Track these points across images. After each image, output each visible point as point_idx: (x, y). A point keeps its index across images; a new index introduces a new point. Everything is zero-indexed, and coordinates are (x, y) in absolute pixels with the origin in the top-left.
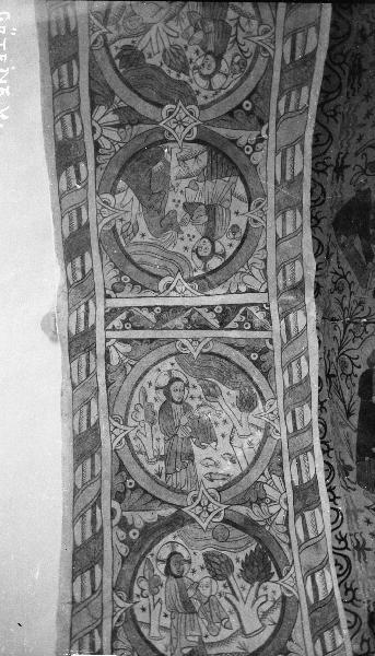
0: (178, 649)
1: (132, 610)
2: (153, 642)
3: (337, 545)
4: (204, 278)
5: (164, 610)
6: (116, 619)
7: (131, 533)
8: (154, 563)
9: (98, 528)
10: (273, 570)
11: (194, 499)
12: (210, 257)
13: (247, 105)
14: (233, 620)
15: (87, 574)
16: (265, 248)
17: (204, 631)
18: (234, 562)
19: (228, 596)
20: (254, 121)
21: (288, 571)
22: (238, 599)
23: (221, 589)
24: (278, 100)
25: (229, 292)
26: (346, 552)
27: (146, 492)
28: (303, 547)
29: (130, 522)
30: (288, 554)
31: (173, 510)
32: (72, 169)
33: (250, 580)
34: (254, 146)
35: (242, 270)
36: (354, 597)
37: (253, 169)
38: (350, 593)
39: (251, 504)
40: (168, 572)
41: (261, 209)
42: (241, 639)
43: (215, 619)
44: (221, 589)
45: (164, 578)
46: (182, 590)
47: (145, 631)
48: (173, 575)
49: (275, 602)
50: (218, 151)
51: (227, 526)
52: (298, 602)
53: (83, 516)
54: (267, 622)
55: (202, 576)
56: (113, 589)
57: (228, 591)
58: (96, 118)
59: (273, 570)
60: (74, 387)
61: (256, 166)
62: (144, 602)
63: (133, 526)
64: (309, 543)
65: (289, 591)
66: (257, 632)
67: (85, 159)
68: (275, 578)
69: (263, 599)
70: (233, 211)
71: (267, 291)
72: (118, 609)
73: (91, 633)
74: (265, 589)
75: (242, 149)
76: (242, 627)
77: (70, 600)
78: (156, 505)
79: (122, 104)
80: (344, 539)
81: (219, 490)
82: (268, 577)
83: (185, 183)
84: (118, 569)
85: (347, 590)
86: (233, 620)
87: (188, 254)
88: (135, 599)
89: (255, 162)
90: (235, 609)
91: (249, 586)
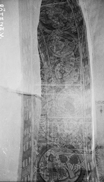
5: (48, 170)
6: (34, 173)
7: (39, 148)
8: (45, 157)
10: (79, 161)
14: (67, 174)
15: (27, 159)
18: (68, 158)
19: (66, 167)
22: (68, 168)
23: (64, 165)
40: (49, 160)
43: (62, 173)
44: (64, 165)
46: (53, 165)
48: (50, 161)
55: (59, 162)
56: (34, 164)
60: (25, 108)
65: (83, 167)
72: (35, 170)
73: (27, 176)
74: (76, 166)
76: (69, 176)
77: (22, 167)
86: (67, 174)
88: (40, 167)
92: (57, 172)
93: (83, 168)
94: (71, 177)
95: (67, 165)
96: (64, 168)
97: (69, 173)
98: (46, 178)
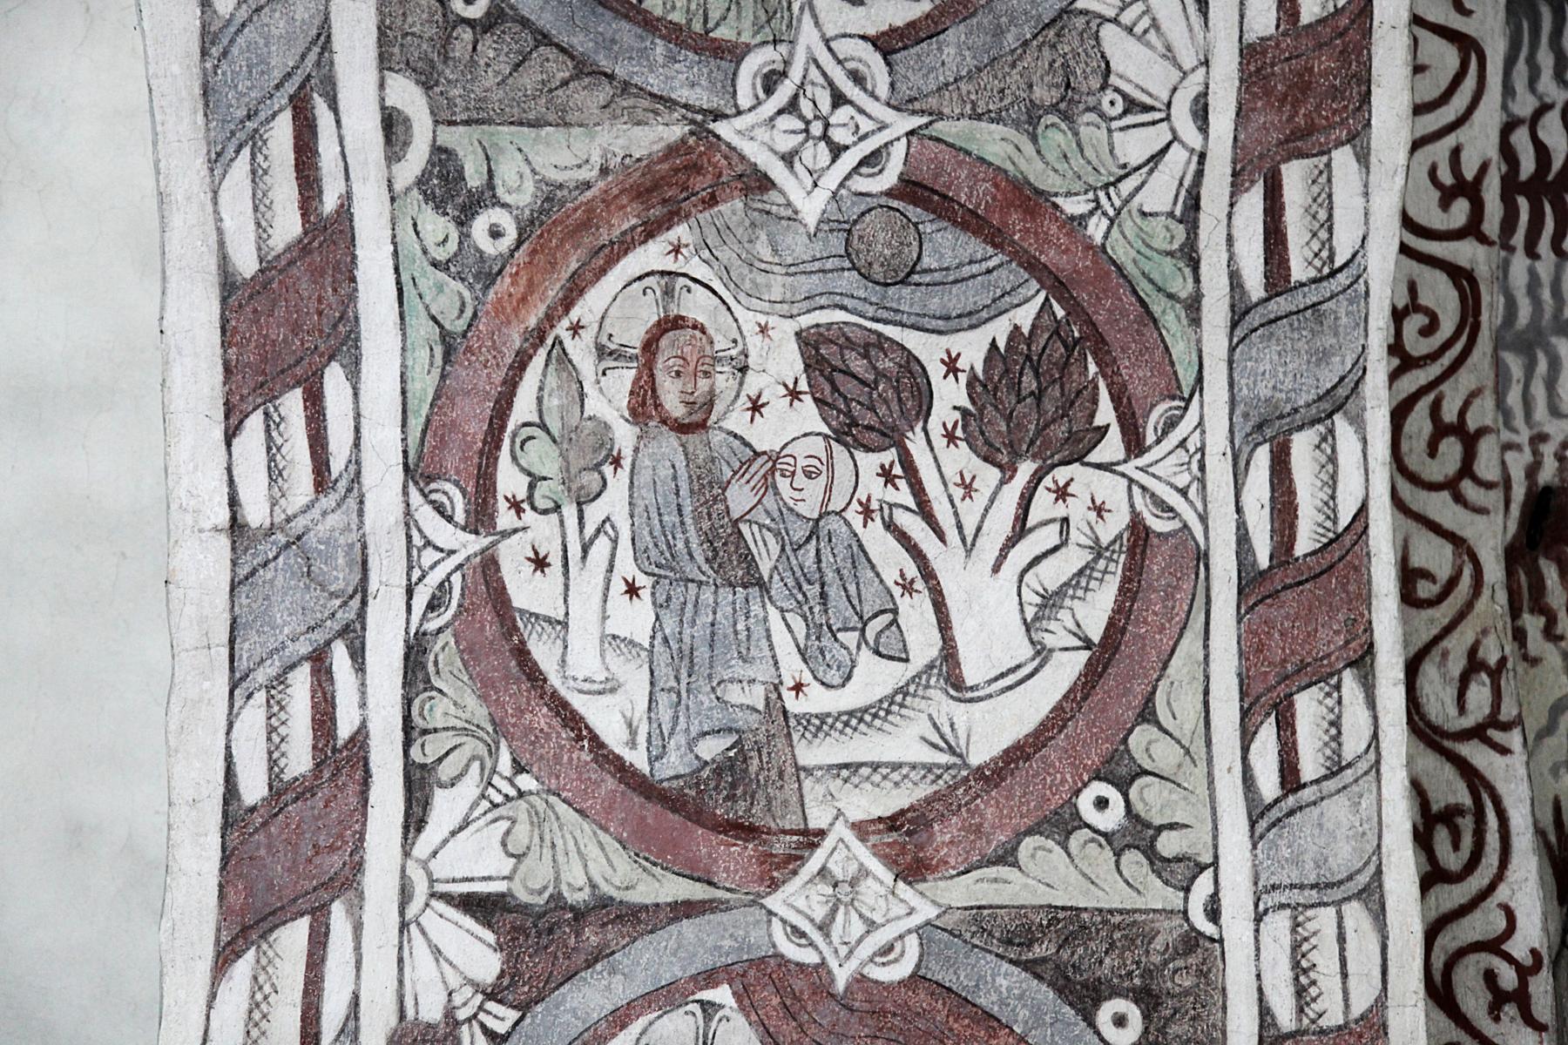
0: (680, 739)
1: (489, 565)
2: (578, 702)
3: (1435, 219)
5: (626, 566)
7: (480, 227)
9: (330, 203)
11: (771, 81)
14: (916, 615)
17: (792, 668)
18: (936, 371)
21: (1171, 424)
23: (874, 487)
26: (1465, 252)
27: (543, 38)
28: (1254, 319)
29: (474, 178)
30: (1179, 349)
31: (677, 132)
33: (1000, 455)
36: (1466, 469)
38: (1451, 450)
39: (1033, 120)
40: (643, 406)
42: (941, 704)
43: (840, 609)
44: (874, 487)
45: (624, 435)
47: (543, 652)
49: (1098, 550)
51: (914, 212)
52: (1203, 557)
53: (256, 141)
54: (1057, 635)
57: (904, 496)
59: (1106, 413)
62: (542, 531)
63: (487, 196)
64: (1281, 305)
66: (1012, 678)
68: (1112, 447)
69: (1048, 538)
72: (429, 556)
73: (319, 660)
74: (1062, 493)
76: (949, 653)
77: (223, 516)
78: (590, 98)
80: (1469, 190)
81: (888, 44)
82: (1079, 447)
84: (424, 384)
85: (1441, 430)
86: (916, 615)
88: (505, 519)
90: (928, 574)
91: (994, 474)
92: (763, 586)
93: (1159, 525)
94: (971, 675)
95: (918, 489)
96: (877, 525)
97: (940, 606)
98: (610, 687)
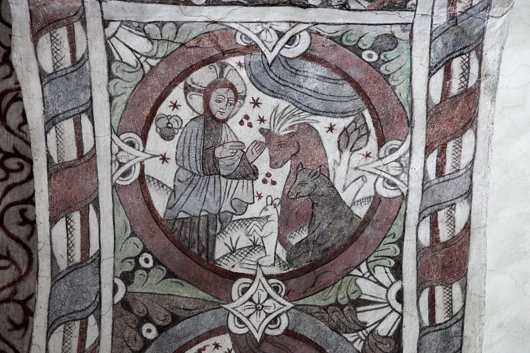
4: (223, 53)
12: (213, 86)
13: (149, 331)
16: (111, 99)
20: (139, 308)
24: (98, 341)
25: (177, 25)
32: (444, 235)
34: (138, 266)
35: (153, 62)
37: (138, 230)
41: (121, 165)
50: (197, 259)
58: (395, 316)
61: (133, 234)
67: (420, 250)
70: (172, 162)
71: (106, 24)
75: (157, 262)
79: (350, 337)
83: (253, 211)
87: (253, 93)
89: (135, 240)
